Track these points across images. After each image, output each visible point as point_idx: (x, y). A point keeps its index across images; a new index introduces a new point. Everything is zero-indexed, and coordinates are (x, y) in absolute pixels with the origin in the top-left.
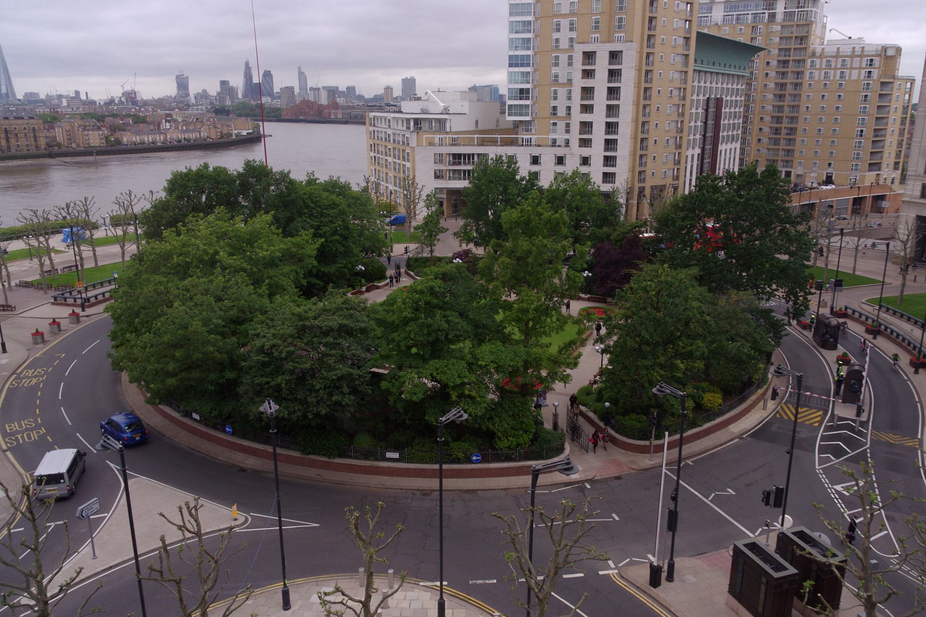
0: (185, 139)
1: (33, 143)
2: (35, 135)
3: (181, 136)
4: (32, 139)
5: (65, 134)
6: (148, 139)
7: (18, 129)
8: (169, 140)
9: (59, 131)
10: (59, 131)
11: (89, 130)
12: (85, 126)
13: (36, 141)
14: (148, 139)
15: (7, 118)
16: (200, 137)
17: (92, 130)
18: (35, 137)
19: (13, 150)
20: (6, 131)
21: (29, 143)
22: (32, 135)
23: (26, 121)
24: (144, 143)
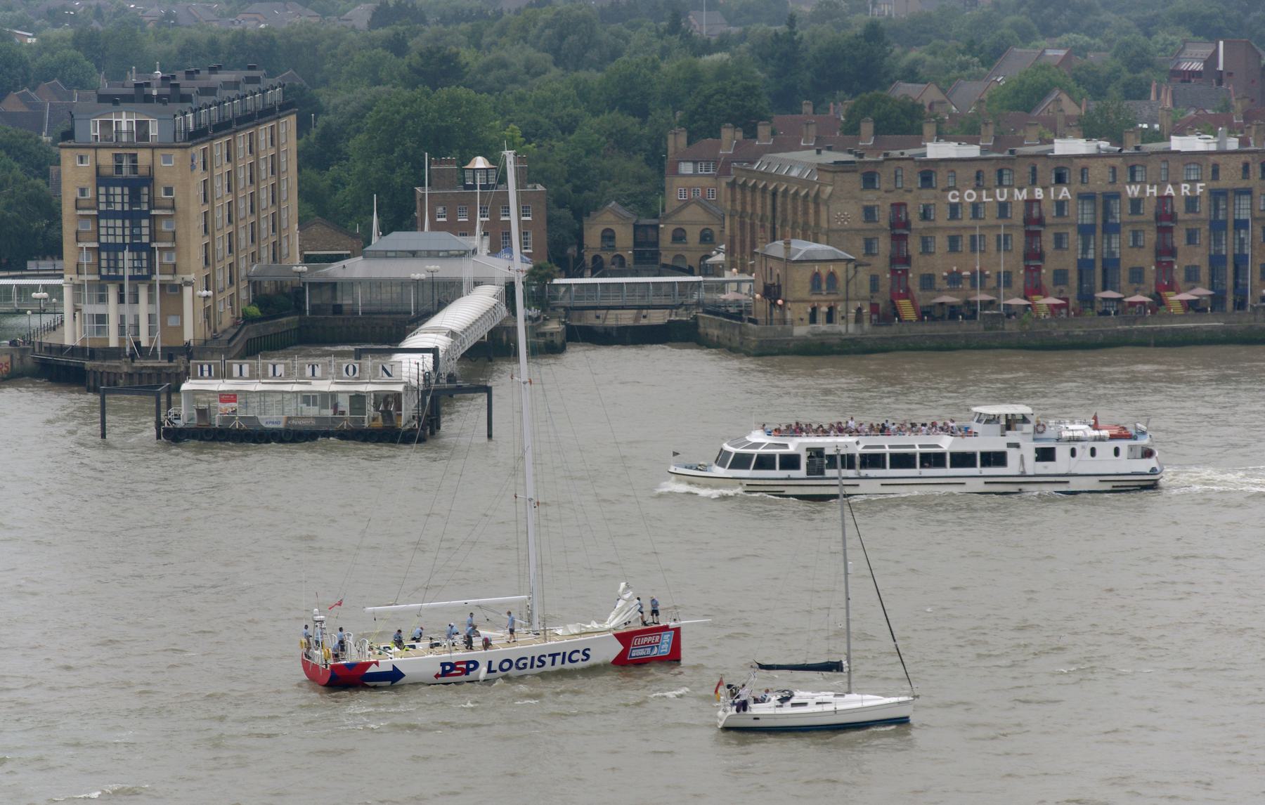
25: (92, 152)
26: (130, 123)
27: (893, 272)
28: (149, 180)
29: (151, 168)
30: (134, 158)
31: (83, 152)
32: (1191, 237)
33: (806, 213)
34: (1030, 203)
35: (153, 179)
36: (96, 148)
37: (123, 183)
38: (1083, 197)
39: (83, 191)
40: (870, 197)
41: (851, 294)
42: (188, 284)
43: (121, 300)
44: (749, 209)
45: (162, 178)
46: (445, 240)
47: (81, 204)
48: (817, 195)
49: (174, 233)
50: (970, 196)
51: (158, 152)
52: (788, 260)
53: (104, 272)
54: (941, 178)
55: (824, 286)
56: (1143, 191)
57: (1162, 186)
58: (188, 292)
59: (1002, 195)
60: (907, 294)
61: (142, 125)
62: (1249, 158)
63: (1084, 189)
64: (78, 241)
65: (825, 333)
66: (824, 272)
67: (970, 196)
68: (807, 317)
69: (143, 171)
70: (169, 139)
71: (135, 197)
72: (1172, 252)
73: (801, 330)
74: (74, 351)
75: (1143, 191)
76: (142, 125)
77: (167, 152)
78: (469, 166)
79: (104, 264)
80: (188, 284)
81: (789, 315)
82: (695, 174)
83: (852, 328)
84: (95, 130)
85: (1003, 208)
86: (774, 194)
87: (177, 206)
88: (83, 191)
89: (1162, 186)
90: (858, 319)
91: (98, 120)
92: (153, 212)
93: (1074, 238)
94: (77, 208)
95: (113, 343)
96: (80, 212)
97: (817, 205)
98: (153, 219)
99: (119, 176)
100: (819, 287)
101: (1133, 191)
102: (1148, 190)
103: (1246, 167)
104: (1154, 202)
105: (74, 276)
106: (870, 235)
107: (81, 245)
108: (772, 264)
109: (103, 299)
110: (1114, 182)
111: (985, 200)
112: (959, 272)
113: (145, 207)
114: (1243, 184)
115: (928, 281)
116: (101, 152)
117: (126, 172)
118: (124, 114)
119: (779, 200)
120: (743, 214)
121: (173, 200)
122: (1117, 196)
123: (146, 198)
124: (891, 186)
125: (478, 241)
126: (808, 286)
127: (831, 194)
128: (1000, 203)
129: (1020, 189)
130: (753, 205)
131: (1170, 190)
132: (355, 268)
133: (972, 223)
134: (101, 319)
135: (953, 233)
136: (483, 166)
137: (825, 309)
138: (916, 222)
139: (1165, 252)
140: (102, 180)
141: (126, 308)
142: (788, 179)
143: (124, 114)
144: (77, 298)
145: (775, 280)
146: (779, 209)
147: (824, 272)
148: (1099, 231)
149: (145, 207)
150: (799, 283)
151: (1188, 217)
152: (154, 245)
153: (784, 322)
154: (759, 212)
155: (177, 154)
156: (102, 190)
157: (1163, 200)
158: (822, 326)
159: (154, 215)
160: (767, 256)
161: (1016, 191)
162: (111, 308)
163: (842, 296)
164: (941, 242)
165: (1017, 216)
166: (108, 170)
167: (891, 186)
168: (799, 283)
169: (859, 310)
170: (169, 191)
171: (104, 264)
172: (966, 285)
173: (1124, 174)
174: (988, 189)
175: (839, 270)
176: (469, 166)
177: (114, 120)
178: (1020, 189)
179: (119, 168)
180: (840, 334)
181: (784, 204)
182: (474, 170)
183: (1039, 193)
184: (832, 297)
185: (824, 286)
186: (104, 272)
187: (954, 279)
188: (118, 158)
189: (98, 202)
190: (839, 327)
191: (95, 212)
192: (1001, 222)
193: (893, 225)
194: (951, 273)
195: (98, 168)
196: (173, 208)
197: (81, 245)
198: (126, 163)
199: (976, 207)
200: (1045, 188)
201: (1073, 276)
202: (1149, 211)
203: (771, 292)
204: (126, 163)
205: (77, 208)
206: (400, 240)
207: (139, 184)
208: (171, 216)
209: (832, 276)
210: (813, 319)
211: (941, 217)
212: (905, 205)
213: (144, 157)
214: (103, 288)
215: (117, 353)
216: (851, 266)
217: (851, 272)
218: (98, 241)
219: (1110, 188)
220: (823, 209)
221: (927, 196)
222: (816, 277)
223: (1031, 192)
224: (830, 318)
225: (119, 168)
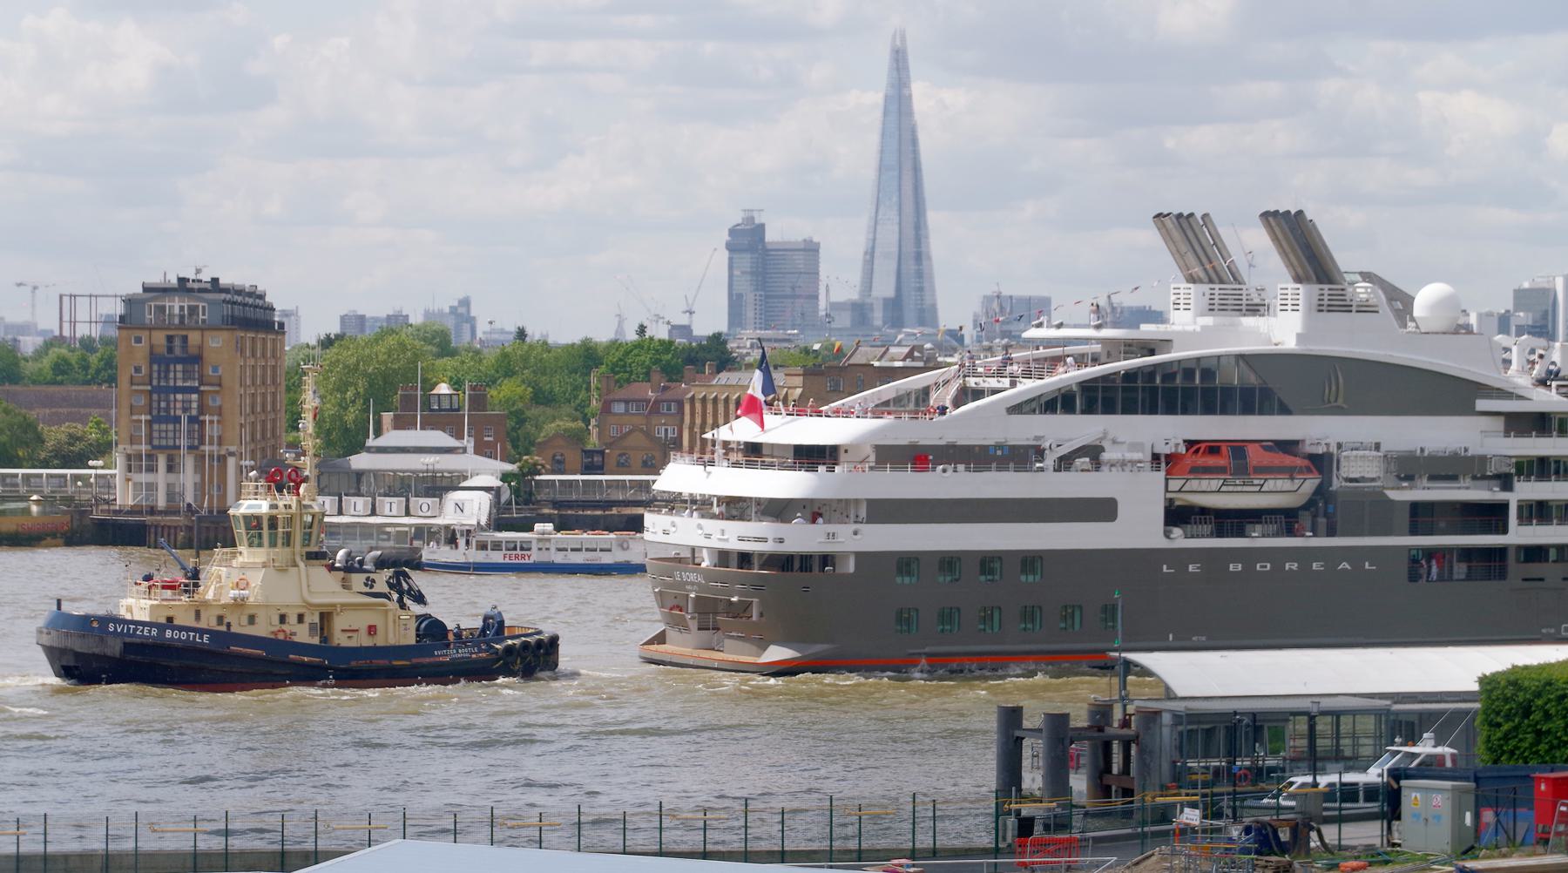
25: (147, 333)
26: (182, 308)
29: (201, 347)
30: (185, 339)
31: (138, 333)
35: (202, 358)
36: (150, 329)
39: (138, 370)
42: (232, 454)
47: (135, 381)
49: (220, 408)
53: (156, 442)
58: (231, 462)
64: (131, 414)
69: (193, 351)
74: (135, 511)
78: (434, 392)
80: (232, 454)
84: (150, 317)
87: (223, 382)
88: (138, 370)
91: (153, 304)
92: (202, 388)
94: (132, 384)
96: (135, 387)
98: (201, 393)
99: (172, 356)
105: (128, 447)
107: (135, 417)
109: (152, 469)
118: (177, 299)
121: (220, 377)
125: (467, 441)
134: (151, 487)
136: (448, 392)
140: (154, 358)
141: (172, 477)
143: (177, 299)
152: (201, 418)
156: (155, 367)
159: (202, 391)
162: (161, 477)
170: (215, 369)
176: (434, 392)
177: (167, 305)
179: (170, 350)
182: (439, 395)
186: (156, 442)
188: (170, 339)
191: (149, 388)
195: (151, 347)
196: (220, 385)
197: (135, 417)
204: (177, 343)
205: (132, 384)
206: (392, 437)
208: (217, 392)
213: (194, 337)
214: (150, 457)
218: (150, 413)
225: (170, 350)
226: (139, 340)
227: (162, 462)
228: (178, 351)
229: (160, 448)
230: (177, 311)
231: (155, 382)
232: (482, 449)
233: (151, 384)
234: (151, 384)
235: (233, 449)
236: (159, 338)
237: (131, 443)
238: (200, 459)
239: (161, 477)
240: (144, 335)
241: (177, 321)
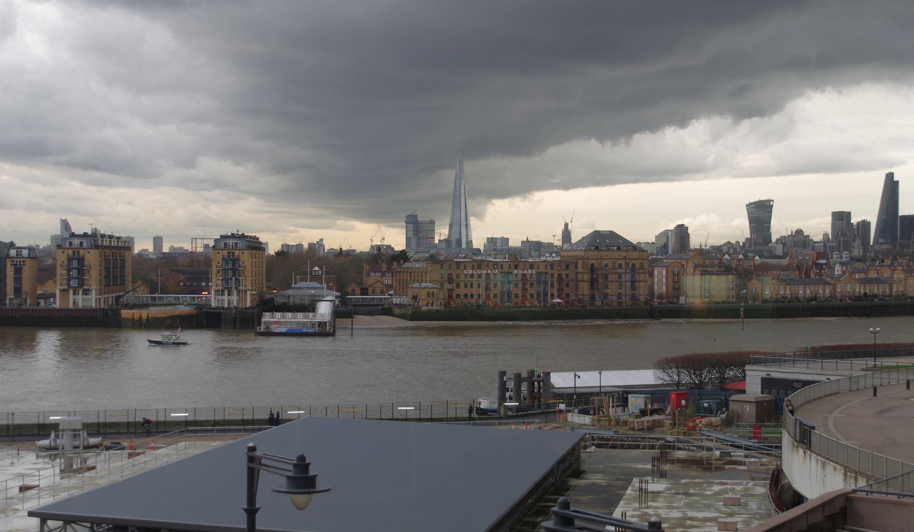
0: (865, 294)
1: (629, 291)
2: (633, 276)
3: (859, 290)
4: (628, 284)
5: (670, 281)
6: (805, 292)
7: (610, 266)
8: (838, 295)
9: (660, 273)
10: (660, 273)
11: (711, 273)
12: (705, 266)
13: (633, 288)
14: (805, 292)
15: (597, 248)
16: (890, 295)
17: (718, 273)
18: (633, 282)
19: (598, 303)
20: (593, 269)
21: (623, 291)
22: (628, 277)
23: (624, 254)
24: (797, 298)
25: (221, 251)
26: (233, 243)
27: (449, 293)
28: (238, 259)
29: (239, 256)
30: (233, 253)
31: (219, 251)
32: (531, 285)
33: (422, 276)
34: (487, 274)
36: (223, 250)
37: (231, 260)
38: (502, 273)
39: (219, 263)
40: (442, 271)
41: (439, 298)
42: (249, 290)
43: (229, 295)
44: (402, 278)
45: (242, 259)
46: (315, 284)
48: (426, 272)
50: (470, 272)
51: (241, 252)
52: (420, 288)
54: (462, 266)
55: (431, 295)
56: (518, 272)
57: (523, 271)
58: (248, 292)
59: (479, 272)
60: (452, 299)
61: (236, 244)
62: (547, 263)
63: (502, 271)
65: (431, 309)
66: (431, 292)
67: (470, 272)
68: (426, 304)
70: (244, 247)
71: (234, 265)
72: (526, 290)
73: (424, 308)
74: (218, 308)
75: (518, 272)
76: (236, 244)
77: (243, 251)
79: (224, 284)
81: (420, 304)
82: (375, 276)
83: (438, 308)
84: (222, 246)
85: (480, 276)
86: (411, 273)
88: (219, 263)
89: (523, 271)
90: (440, 306)
92: (239, 269)
93: (499, 285)
95: (226, 306)
97: (426, 274)
100: (429, 295)
101: (515, 271)
102: (520, 272)
103: (546, 265)
104: (521, 275)
106: (442, 282)
108: (414, 290)
110: (510, 269)
111: (474, 273)
112: (465, 294)
113: (237, 267)
114: (545, 271)
115: (458, 296)
116: (224, 251)
117: (231, 257)
119: (412, 274)
120: (400, 279)
122: (511, 273)
123: (237, 265)
124: (448, 268)
125: (324, 285)
126: (427, 295)
127: (431, 270)
128: (478, 274)
129: (484, 270)
130: (403, 277)
131: (525, 272)
132: (290, 292)
133: (471, 279)
134: (223, 300)
135: (465, 282)
137: (431, 302)
138: (455, 279)
139: (524, 289)
140: (224, 259)
142: (415, 268)
144: (216, 294)
145: (415, 294)
146: (412, 277)
147: (431, 292)
148: (506, 283)
149: (237, 267)
150: (423, 295)
151: (531, 279)
153: (419, 306)
154: (405, 278)
155: (246, 252)
156: (224, 262)
157: (524, 275)
158: (430, 307)
160: (412, 288)
161: (483, 271)
162: (226, 297)
163: (436, 298)
164: (462, 285)
165: (484, 277)
166: (226, 256)
167: (448, 268)
168: (423, 295)
169: (441, 303)
170: (243, 263)
171: (224, 284)
172: (469, 297)
173: (513, 267)
174: (475, 270)
175: (435, 291)
178: (484, 270)
180: (435, 310)
181: (414, 276)
183: (489, 272)
184: (434, 299)
185: (431, 295)
186: (224, 286)
187: (466, 296)
188: (229, 253)
189: (223, 266)
190: (435, 307)
192: (479, 279)
193: (449, 279)
194: (465, 294)
195: (223, 255)
196: (245, 268)
198: (231, 254)
199: (472, 276)
200: (491, 270)
201: (499, 296)
202: (520, 278)
203: (415, 298)
206: (301, 284)
207: (236, 260)
209: (433, 293)
210: (427, 306)
211: (462, 278)
212: (452, 274)
213: (237, 253)
214: (223, 291)
215: (228, 308)
216: (438, 290)
217: (439, 292)
218: (222, 277)
219: (509, 271)
220: (428, 275)
221: (458, 271)
222: (429, 292)
223: (487, 271)
224: (432, 306)
225: (229, 256)
226: (219, 253)
227: (226, 292)
228: (231, 257)
229: (226, 288)
230: (231, 244)
231: (224, 267)
232: (329, 288)
233: (222, 267)
234: (222, 267)
235: (249, 288)
236: (225, 253)
237: (217, 287)
238: (238, 291)
239: (226, 297)
240: (221, 252)
241: (231, 247)
